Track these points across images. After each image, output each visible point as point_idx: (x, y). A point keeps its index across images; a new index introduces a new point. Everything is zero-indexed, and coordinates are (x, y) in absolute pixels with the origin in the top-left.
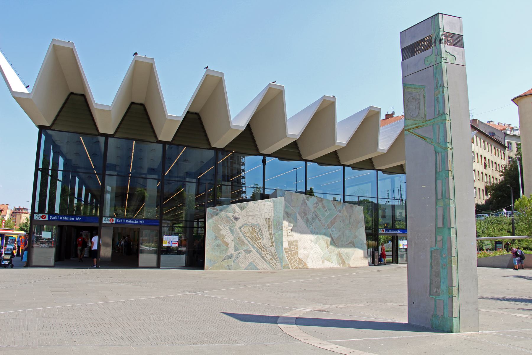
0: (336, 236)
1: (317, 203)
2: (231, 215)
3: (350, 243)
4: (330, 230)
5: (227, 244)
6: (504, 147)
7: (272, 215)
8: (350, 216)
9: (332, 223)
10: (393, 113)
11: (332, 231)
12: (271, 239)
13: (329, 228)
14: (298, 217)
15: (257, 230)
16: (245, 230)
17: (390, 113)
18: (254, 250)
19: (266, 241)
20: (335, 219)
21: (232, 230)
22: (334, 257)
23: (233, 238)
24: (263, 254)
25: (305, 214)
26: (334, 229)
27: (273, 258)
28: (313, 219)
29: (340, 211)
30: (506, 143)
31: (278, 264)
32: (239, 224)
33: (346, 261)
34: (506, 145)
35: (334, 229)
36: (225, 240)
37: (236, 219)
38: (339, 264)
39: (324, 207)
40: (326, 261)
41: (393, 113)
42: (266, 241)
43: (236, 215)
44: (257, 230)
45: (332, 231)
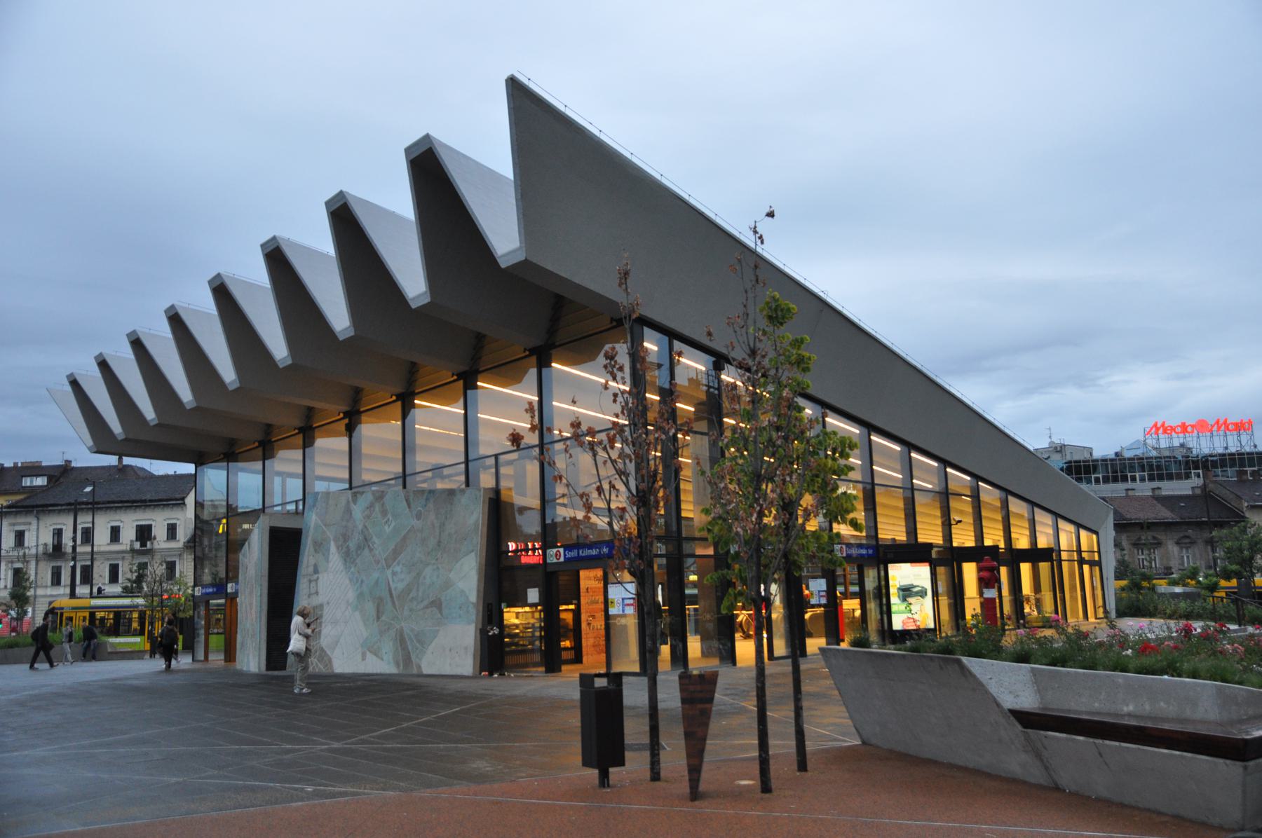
0: (401, 586)
3: (432, 604)
4: (389, 572)
8: (442, 525)
11: (394, 574)
13: (389, 566)
14: (333, 548)
20: (404, 539)
22: (388, 647)
25: (345, 541)
26: (398, 569)
28: (360, 547)
29: (419, 516)
33: (413, 657)
35: (398, 569)
38: (398, 665)
40: (368, 654)
45: (394, 574)
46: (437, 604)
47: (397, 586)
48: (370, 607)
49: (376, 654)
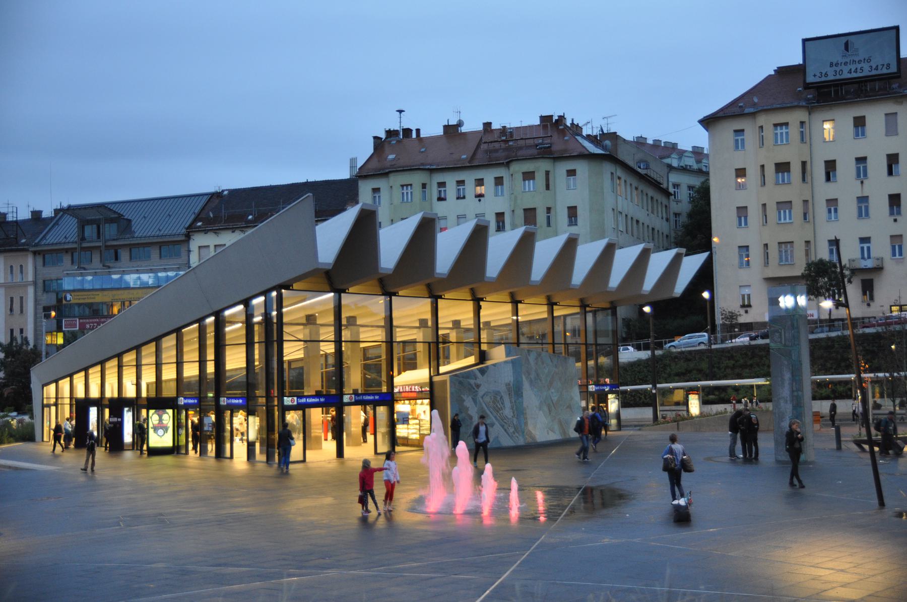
1: (536, 359)
2: (472, 382)
5: (471, 418)
6: (667, 194)
7: (511, 379)
9: (551, 383)
10: (460, 124)
12: (512, 408)
15: (499, 398)
16: (487, 399)
17: (453, 122)
18: (497, 423)
19: (508, 412)
21: (475, 401)
22: (556, 427)
23: (476, 409)
24: (506, 426)
25: (529, 374)
27: (516, 430)
29: (556, 366)
30: (670, 184)
31: (520, 437)
32: (481, 391)
34: (671, 190)
36: (469, 412)
37: (478, 386)
39: (543, 363)
41: (460, 124)
42: (508, 412)
43: (478, 382)
44: (499, 398)
46: (569, 407)
47: (555, 399)
48: (545, 409)
49: (553, 431)
